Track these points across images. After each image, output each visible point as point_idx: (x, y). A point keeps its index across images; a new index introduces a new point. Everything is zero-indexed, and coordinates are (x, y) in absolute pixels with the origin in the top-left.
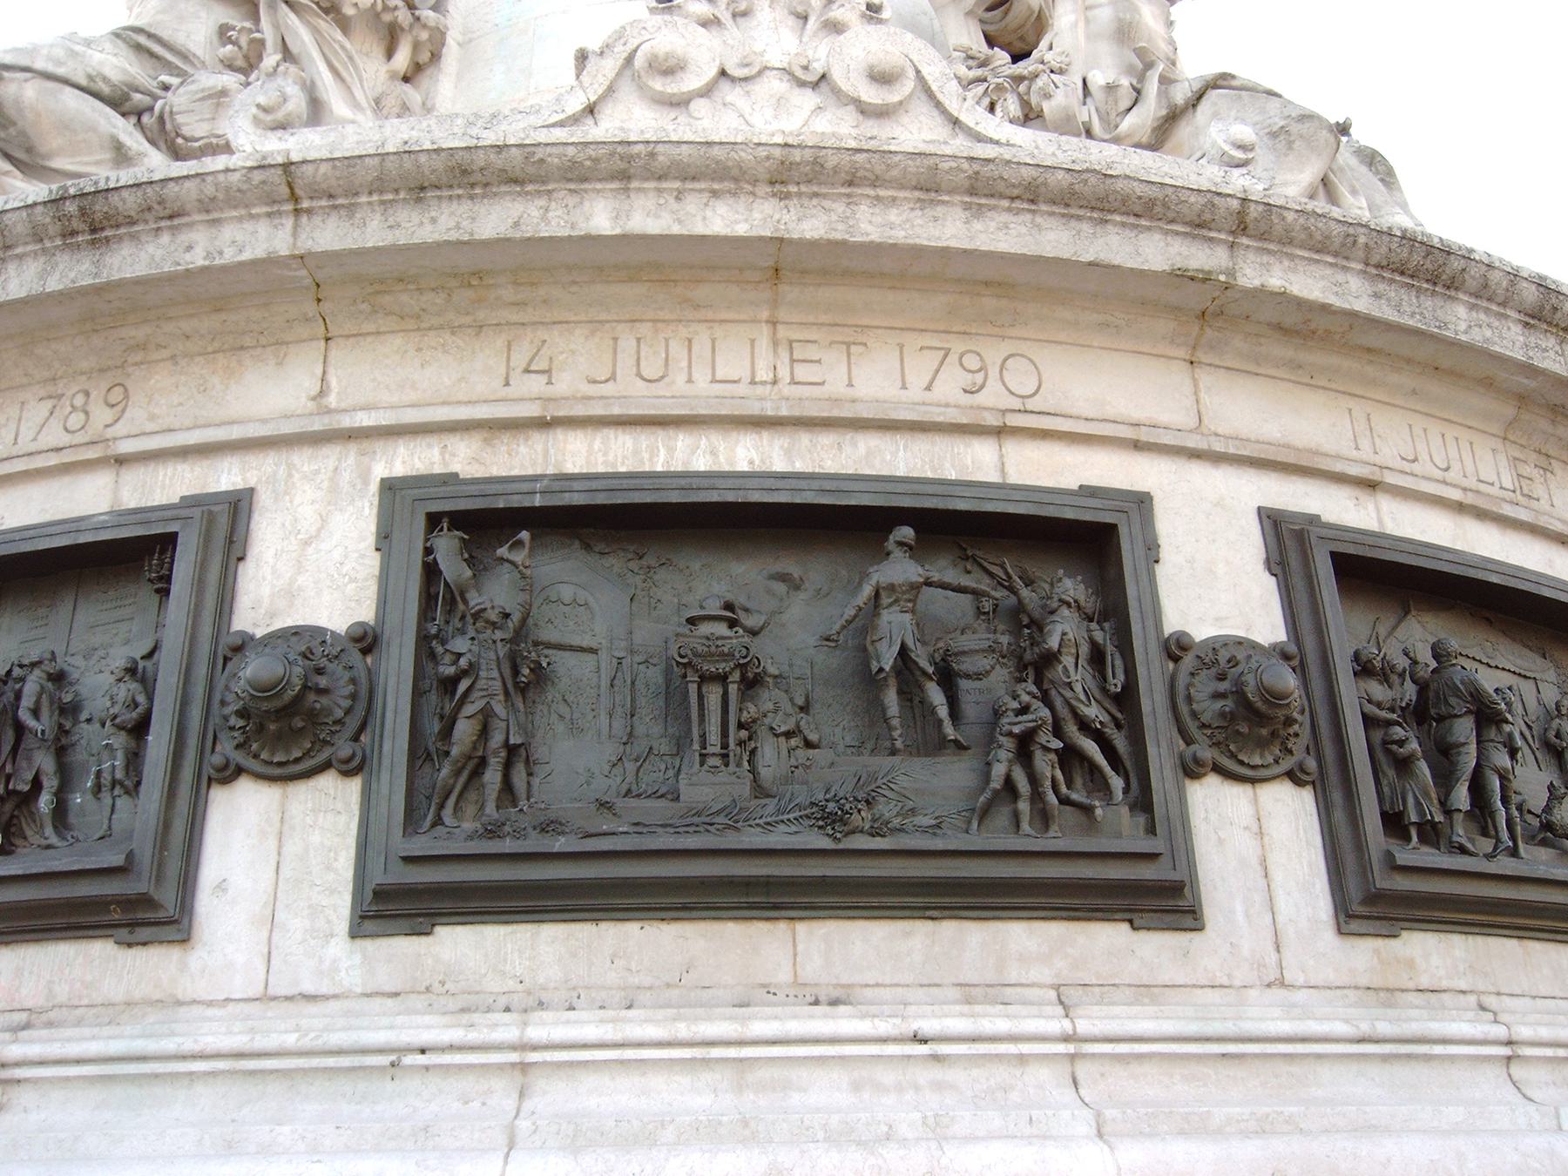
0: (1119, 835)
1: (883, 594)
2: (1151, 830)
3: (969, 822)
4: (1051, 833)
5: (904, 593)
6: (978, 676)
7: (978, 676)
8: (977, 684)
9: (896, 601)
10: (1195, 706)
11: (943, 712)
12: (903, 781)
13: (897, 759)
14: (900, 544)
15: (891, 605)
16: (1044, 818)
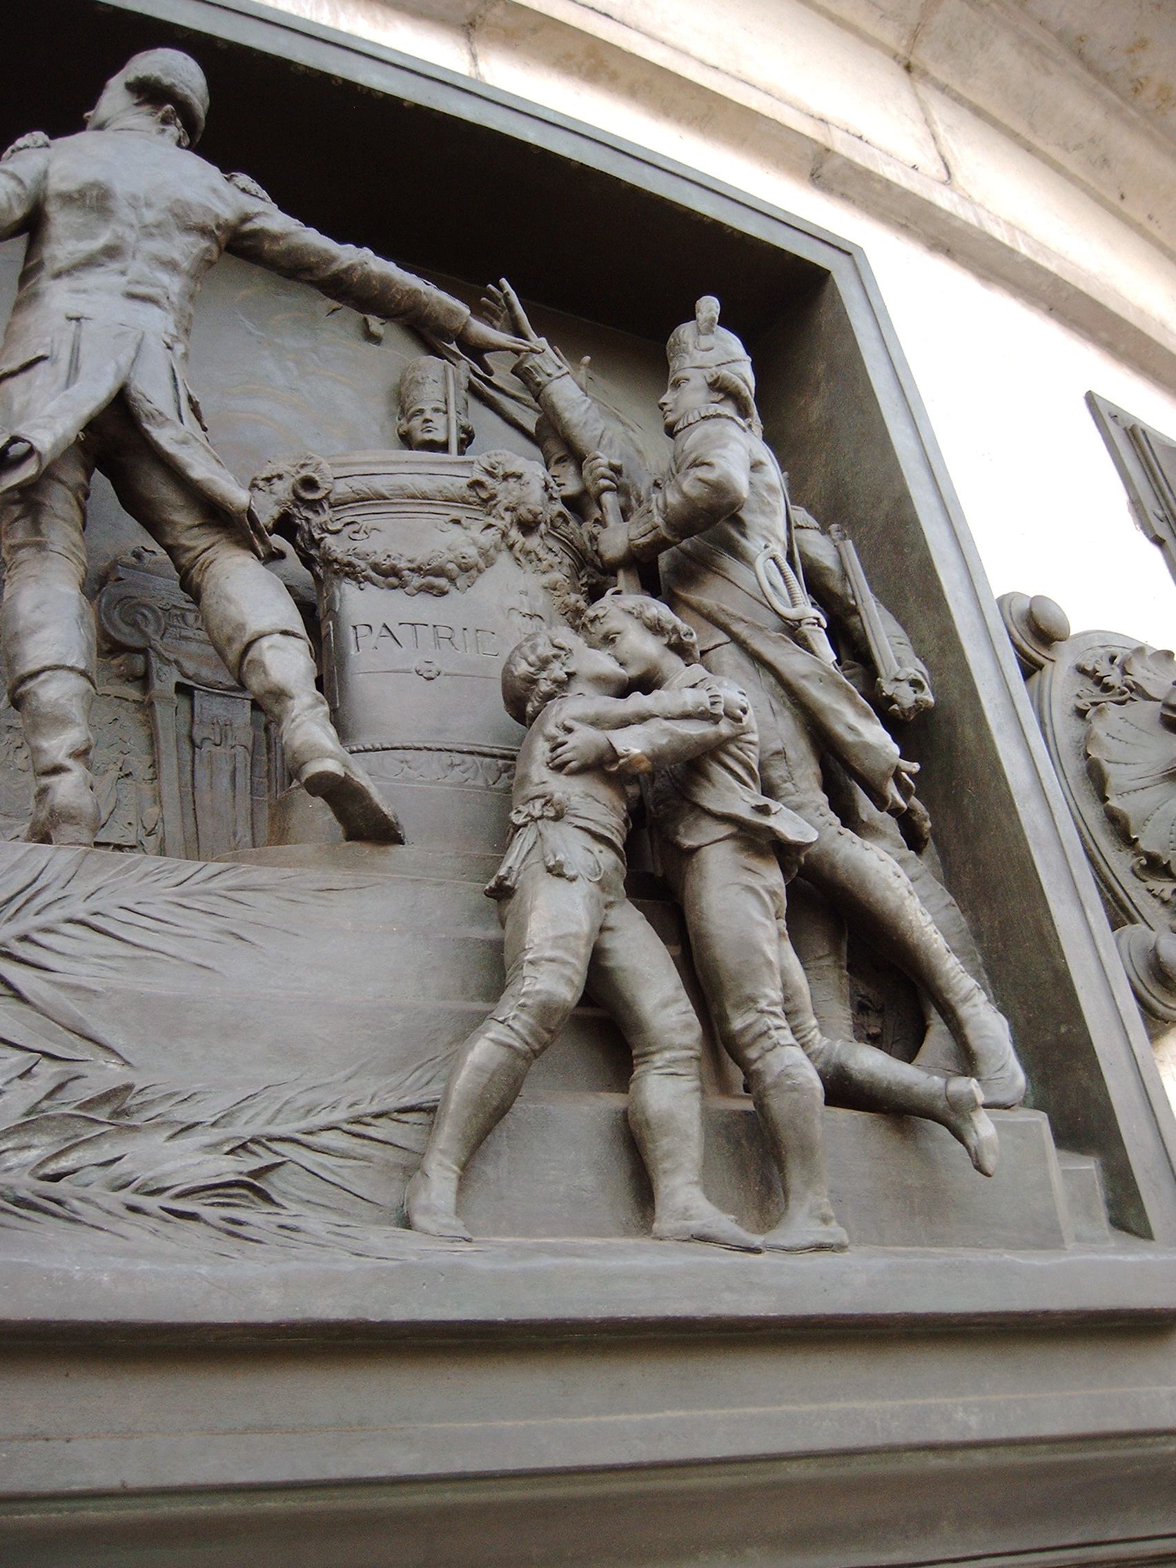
0: (1048, 1236)
1: (60, 220)
2: (1126, 1213)
3: (412, 1168)
4: (801, 1224)
5: (148, 231)
6: (435, 579)
7: (435, 579)
8: (424, 608)
9: (112, 252)
10: (1113, 802)
11: (287, 663)
12: (79, 960)
13: (57, 859)
14: (150, 93)
15: (89, 263)
16: (757, 1153)
